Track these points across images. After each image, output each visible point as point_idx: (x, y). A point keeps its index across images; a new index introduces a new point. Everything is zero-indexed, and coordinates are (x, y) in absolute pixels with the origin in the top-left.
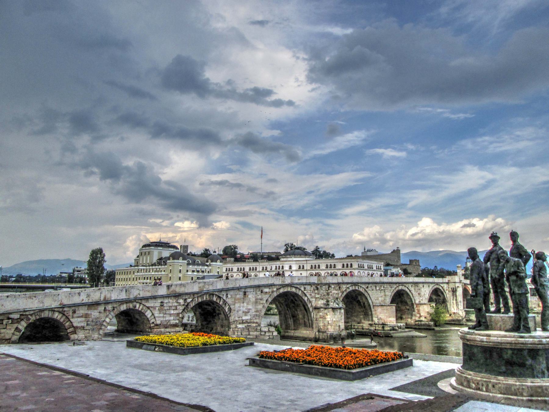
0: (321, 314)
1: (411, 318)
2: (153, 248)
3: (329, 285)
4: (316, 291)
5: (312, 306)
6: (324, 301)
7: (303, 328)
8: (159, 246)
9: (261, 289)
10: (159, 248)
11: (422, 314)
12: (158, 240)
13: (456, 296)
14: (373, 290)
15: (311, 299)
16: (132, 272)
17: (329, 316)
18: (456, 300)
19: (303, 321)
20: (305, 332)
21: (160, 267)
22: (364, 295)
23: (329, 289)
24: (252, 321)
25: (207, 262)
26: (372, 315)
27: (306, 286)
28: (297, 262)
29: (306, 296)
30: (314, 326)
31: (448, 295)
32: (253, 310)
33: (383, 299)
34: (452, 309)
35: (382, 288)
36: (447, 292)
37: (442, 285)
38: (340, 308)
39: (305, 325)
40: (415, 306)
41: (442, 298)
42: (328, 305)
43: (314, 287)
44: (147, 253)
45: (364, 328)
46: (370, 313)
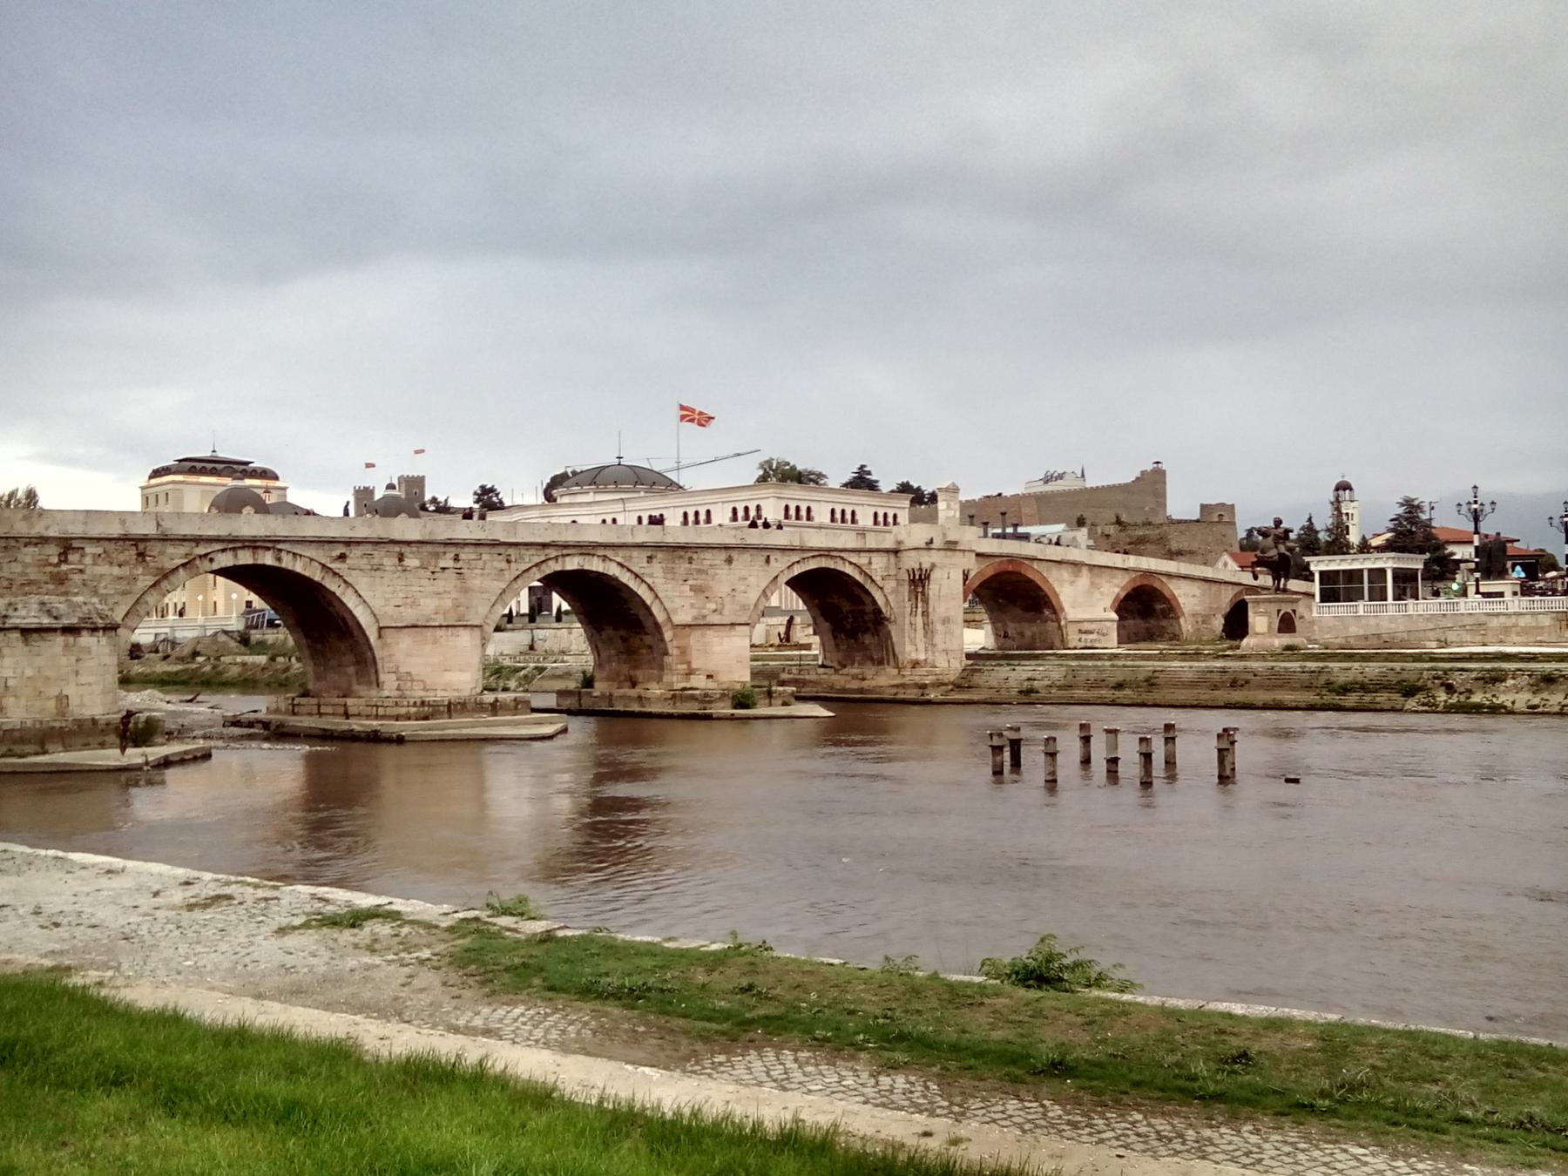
1: (659, 680)
3: (67, 545)
8: (203, 472)
11: (694, 666)
12: (206, 454)
13: (926, 601)
14: (378, 568)
18: (925, 614)
22: (319, 587)
28: (596, 509)
31: (889, 595)
33: (448, 603)
34: (909, 648)
35: (450, 564)
36: (890, 585)
37: (862, 560)
40: (668, 635)
41: (869, 608)
45: (351, 710)
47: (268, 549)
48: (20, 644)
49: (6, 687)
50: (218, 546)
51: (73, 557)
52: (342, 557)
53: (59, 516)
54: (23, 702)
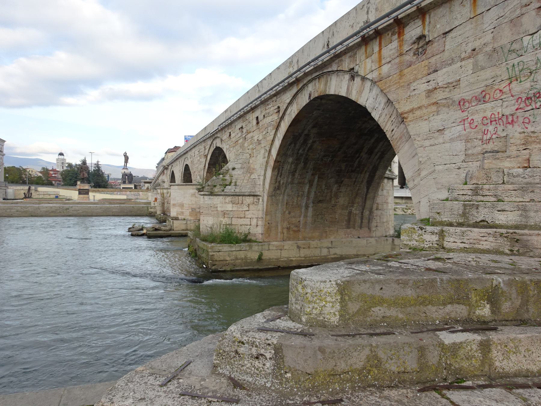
19: (346, 212)
39: (349, 224)
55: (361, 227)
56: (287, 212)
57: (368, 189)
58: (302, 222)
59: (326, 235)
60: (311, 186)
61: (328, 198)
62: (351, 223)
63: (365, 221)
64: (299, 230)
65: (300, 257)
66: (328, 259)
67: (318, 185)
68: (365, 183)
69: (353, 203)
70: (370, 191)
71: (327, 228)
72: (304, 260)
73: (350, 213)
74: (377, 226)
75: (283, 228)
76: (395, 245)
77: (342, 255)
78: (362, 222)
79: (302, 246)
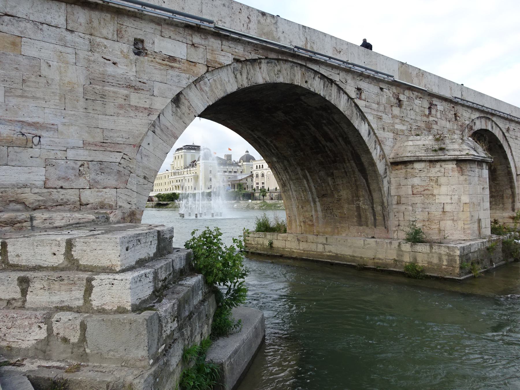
0: (416, 181)
2: (185, 151)
4: (396, 111)
5: (384, 156)
6: (428, 140)
7: (354, 229)
9: (134, 29)
10: (192, 151)
12: (191, 144)
15: (381, 134)
16: (167, 177)
17: (444, 189)
20: (359, 242)
21: (191, 169)
22: (501, 147)
23: (430, 113)
24: (58, 195)
25: (240, 162)
26: (513, 195)
27: (364, 85)
29: (364, 118)
30: (392, 222)
32: (74, 136)
38: (480, 162)
39: (361, 221)
42: (442, 149)
43: (389, 93)
44: (180, 157)
46: (509, 192)
47: (489, 119)
48: (456, 174)
49: (444, 212)
50: (477, 115)
51: (433, 112)
52: (508, 130)
53: (429, 77)
54: (460, 224)
55: (375, 226)
56: (300, 207)
57: (367, 180)
58: (314, 217)
59: (338, 232)
60: (308, 181)
61: (329, 192)
62: (363, 219)
63: (379, 218)
64: (313, 224)
65: (299, 249)
66: (324, 255)
67: (313, 179)
68: (357, 173)
69: (358, 197)
70: (370, 181)
71: (338, 224)
72: (303, 253)
73: (358, 208)
74: (399, 225)
75: (300, 222)
76: (402, 251)
77: (337, 254)
78: (375, 219)
79: (302, 240)
